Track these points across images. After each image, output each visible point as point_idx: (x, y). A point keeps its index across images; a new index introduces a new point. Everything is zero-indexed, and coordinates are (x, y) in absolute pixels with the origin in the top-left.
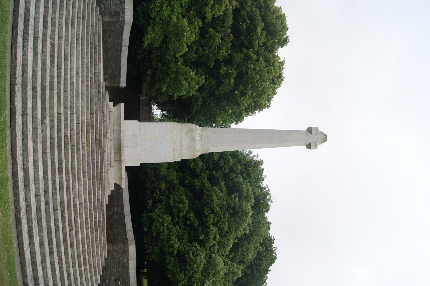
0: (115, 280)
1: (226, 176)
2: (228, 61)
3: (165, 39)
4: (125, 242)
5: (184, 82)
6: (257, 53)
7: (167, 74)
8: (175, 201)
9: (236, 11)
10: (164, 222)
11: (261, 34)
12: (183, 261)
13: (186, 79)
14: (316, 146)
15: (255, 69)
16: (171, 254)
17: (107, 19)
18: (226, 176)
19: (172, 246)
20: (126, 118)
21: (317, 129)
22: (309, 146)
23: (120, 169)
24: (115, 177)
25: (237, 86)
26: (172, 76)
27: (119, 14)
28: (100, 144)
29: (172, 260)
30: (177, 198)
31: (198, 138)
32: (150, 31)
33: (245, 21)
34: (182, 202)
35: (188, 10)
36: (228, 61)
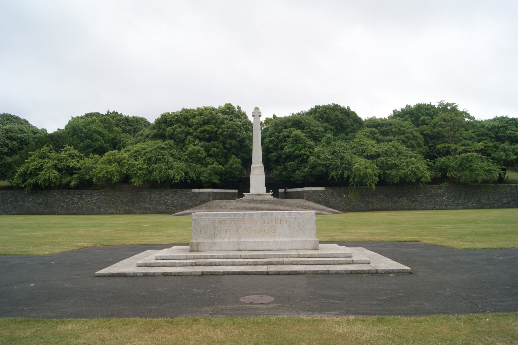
0: (320, 196)
1: (281, 141)
2: (224, 143)
3: (216, 173)
4: (304, 192)
5: (235, 166)
6: (219, 128)
7: (232, 172)
8: (290, 168)
9: (201, 140)
10: (298, 175)
11: (210, 127)
12: (313, 167)
13: (234, 164)
14: (260, 113)
15: (227, 131)
16: (311, 172)
17: (211, 198)
18: (281, 141)
19: (307, 172)
20: (249, 192)
21: (253, 113)
22: (260, 116)
23: (266, 194)
24: (269, 196)
25: (236, 139)
26: (232, 170)
27: (209, 194)
28: (255, 201)
29: (313, 171)
30: (289, 167)
31: (256, 165)
32: (214, 181)
33: (205, 135)
34: (291, 164)
35: (202, 164)
36: (224, 143)
